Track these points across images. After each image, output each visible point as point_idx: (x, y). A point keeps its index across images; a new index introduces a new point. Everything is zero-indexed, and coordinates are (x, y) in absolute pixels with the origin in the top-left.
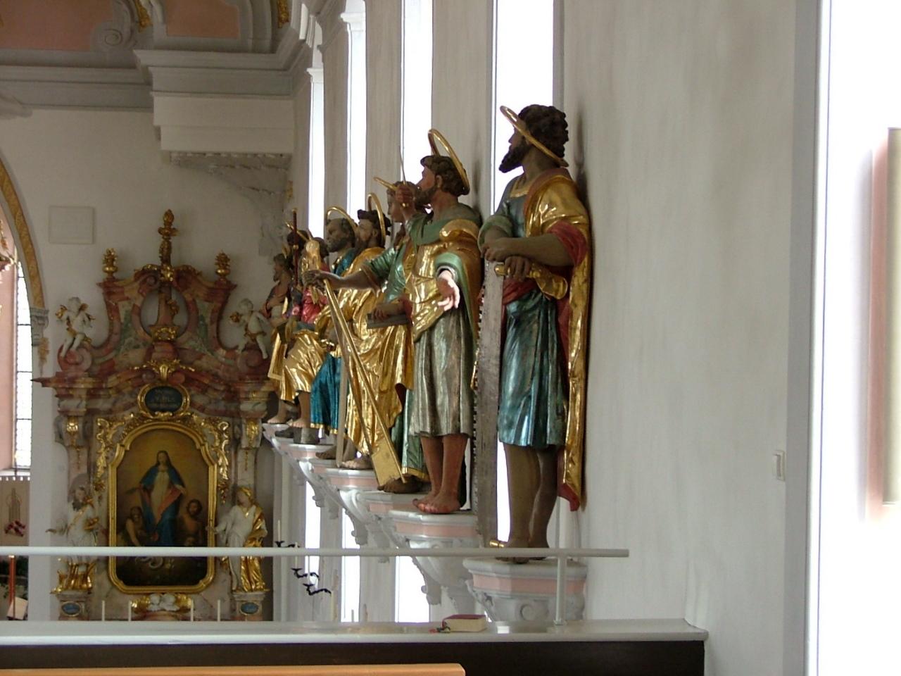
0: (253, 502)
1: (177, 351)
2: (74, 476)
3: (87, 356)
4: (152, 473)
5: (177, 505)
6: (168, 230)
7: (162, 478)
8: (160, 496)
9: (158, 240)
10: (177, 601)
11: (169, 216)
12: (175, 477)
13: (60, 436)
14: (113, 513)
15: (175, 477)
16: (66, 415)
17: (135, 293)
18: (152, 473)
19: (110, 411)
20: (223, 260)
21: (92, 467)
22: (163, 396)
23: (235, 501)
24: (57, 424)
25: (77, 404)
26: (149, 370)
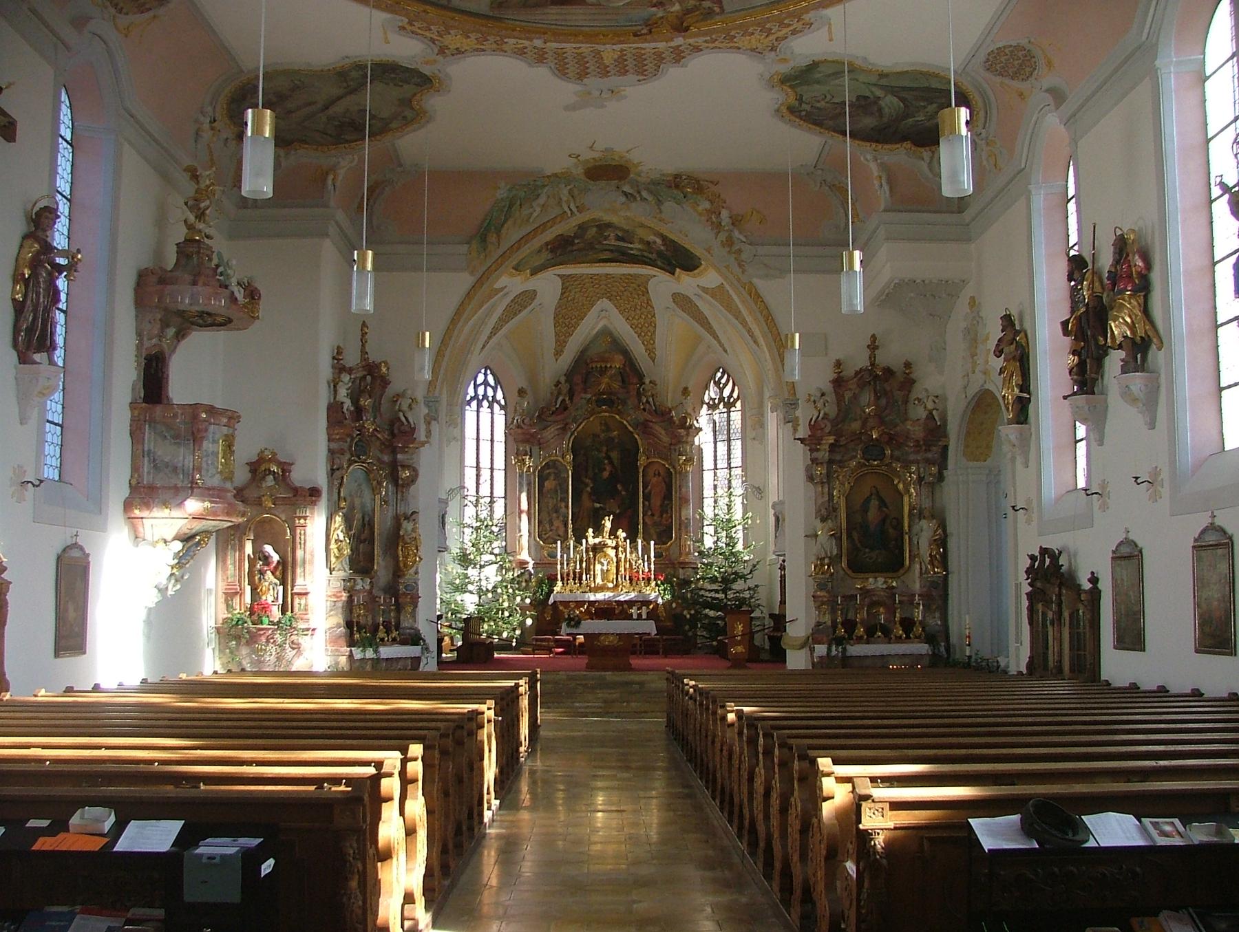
0: (933, 517)
1: (882, 422)
2: (820, 502)
3: (829, 425)
4: (868, 500)
5: (884, 521)
6: (873, 346)
7: (874, 503)
8: (873, 514)
9: (868, 352)
10: (885, 582)
11: (874, 337)
12: (883, 503)
13: (810, 478)
14: (844, 526)
15: (883, 503)
16: (814, 461)
17: (854, 386)
18: (868, 500)
19: (840, 461)
20: (908, 365)
21: (831, 496)
22: (873, 450)
23: (921, 516)
24: (808, 469)
25: (823, 454)
26: (866, 433)
